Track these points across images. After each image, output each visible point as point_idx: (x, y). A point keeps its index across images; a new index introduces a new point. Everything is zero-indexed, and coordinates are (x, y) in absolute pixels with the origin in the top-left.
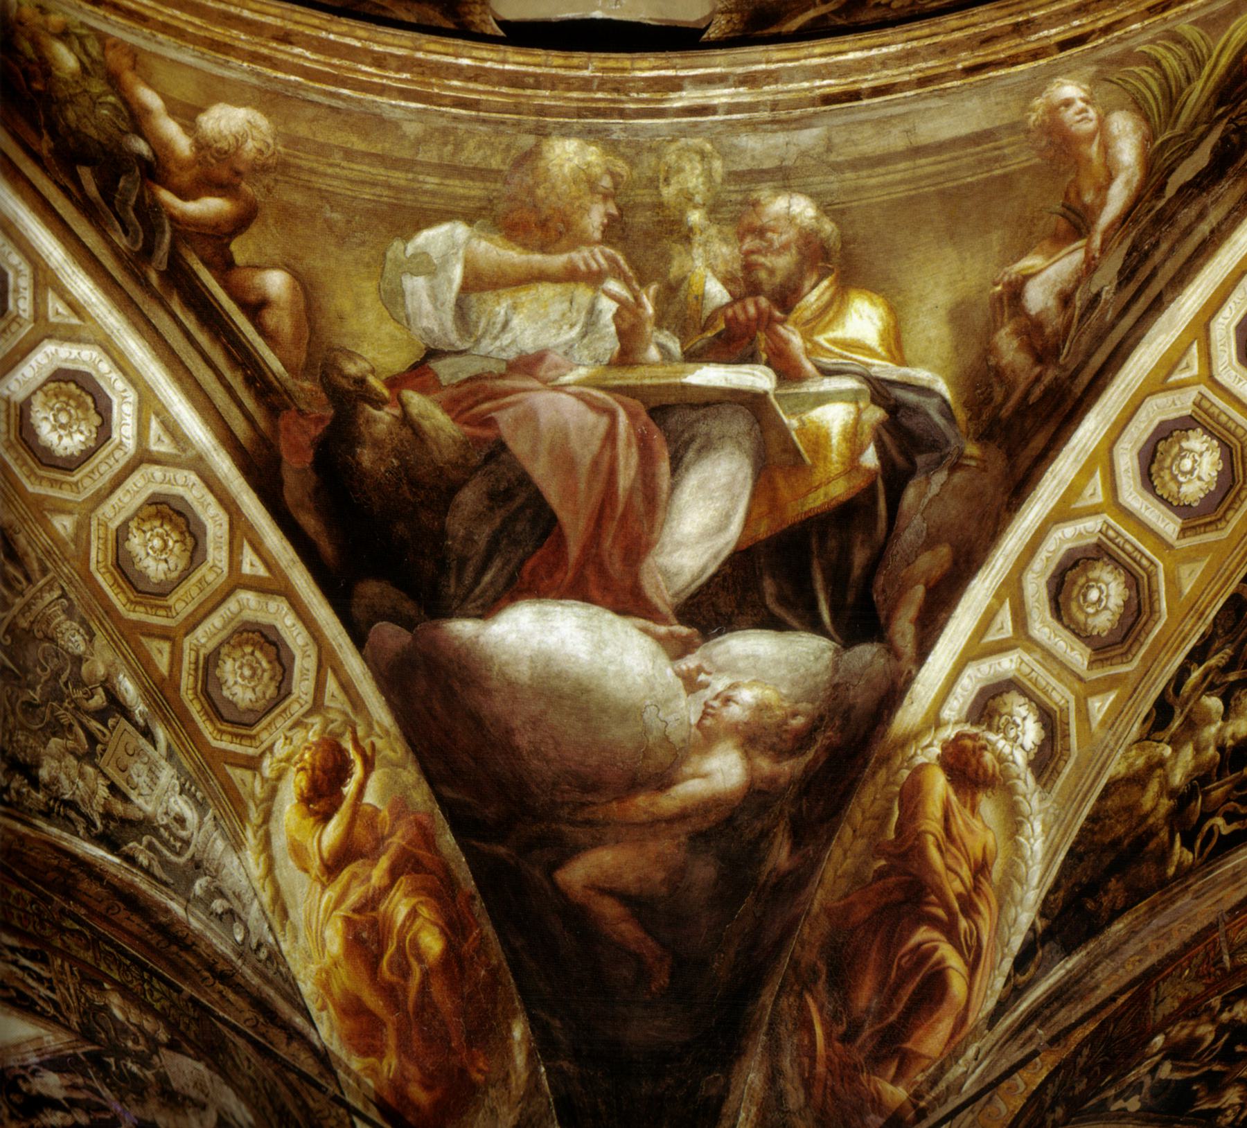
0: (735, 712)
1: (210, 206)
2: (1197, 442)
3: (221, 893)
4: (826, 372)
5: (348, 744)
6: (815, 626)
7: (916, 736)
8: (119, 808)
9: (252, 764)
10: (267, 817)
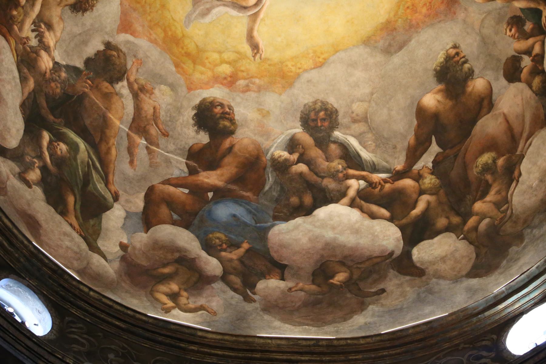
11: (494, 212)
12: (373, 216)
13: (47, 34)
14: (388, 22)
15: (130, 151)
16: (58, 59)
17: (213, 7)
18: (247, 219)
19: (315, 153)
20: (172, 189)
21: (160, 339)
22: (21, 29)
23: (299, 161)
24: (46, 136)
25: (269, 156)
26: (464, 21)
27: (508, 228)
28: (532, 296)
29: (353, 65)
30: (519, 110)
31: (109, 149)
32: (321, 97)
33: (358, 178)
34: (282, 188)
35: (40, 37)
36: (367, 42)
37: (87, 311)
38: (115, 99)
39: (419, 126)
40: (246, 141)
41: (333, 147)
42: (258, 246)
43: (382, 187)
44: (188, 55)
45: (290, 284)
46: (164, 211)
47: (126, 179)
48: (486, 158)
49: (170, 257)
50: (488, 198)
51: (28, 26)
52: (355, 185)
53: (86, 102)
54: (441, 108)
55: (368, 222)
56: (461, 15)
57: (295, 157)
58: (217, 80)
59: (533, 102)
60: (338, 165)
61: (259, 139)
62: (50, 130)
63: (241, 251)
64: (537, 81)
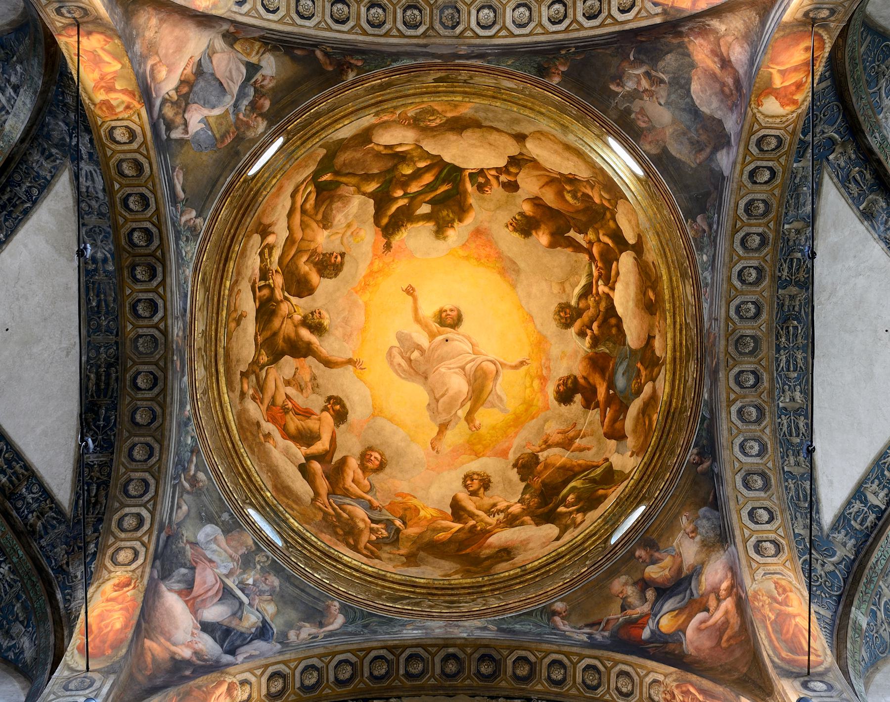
0: (196, 646)
1: (187, 485)
2: (315, 674)
3: (71, 595)
4: (257, 610)
5: (133, 582)
6: (222, 646)
7: (230, 674)
8: (65, 566)
9: (110, 572)
10: (103, 583)
11: (596, 188)
12: (618, 274)
13: (498, 507)
14: (499, 273)
15: (581, 450)
16: (517, 500)
17: (497, 394)
18: (625, 364)
19: (586, 317)
20: (607, 420)
21: (667, 427)
22: (490, 525)
23: (591, 329)
24: (562, 509)
25: (589, 351)
26: (489, 222)
27: (600, 178)
28: (615, 160)
29: (529, 295)
30: (534, 179)
31: (580, 465)
32: (551, 315)
33: (597, 286)
34: (607, 340)
35: (499, 512)
36: (514, 286)
37: (646, 481)
38: (549, 461)
39: (560, 246)
40: (581, 368)
41: (581, 305)
42: (639, 355)
43: (600, 268)
44: (526, 410)
45: (657, 331)
46: (618, 425)
47: (597, 453)
48: (568, 197)
49: (641, 421)
50: (591, 194)
51: (492, 520)
52: (602, 288)
53: (547, 481)
54: (547, 232)
55: (621, 277)
56: (486, 225)
57: (589, 331)
58: (542, 390)
59: (526, 171)
60: (591, 301)
61: (579, 358)
62: (558, 506)
63: (642, 368)
64: (513, 170)
